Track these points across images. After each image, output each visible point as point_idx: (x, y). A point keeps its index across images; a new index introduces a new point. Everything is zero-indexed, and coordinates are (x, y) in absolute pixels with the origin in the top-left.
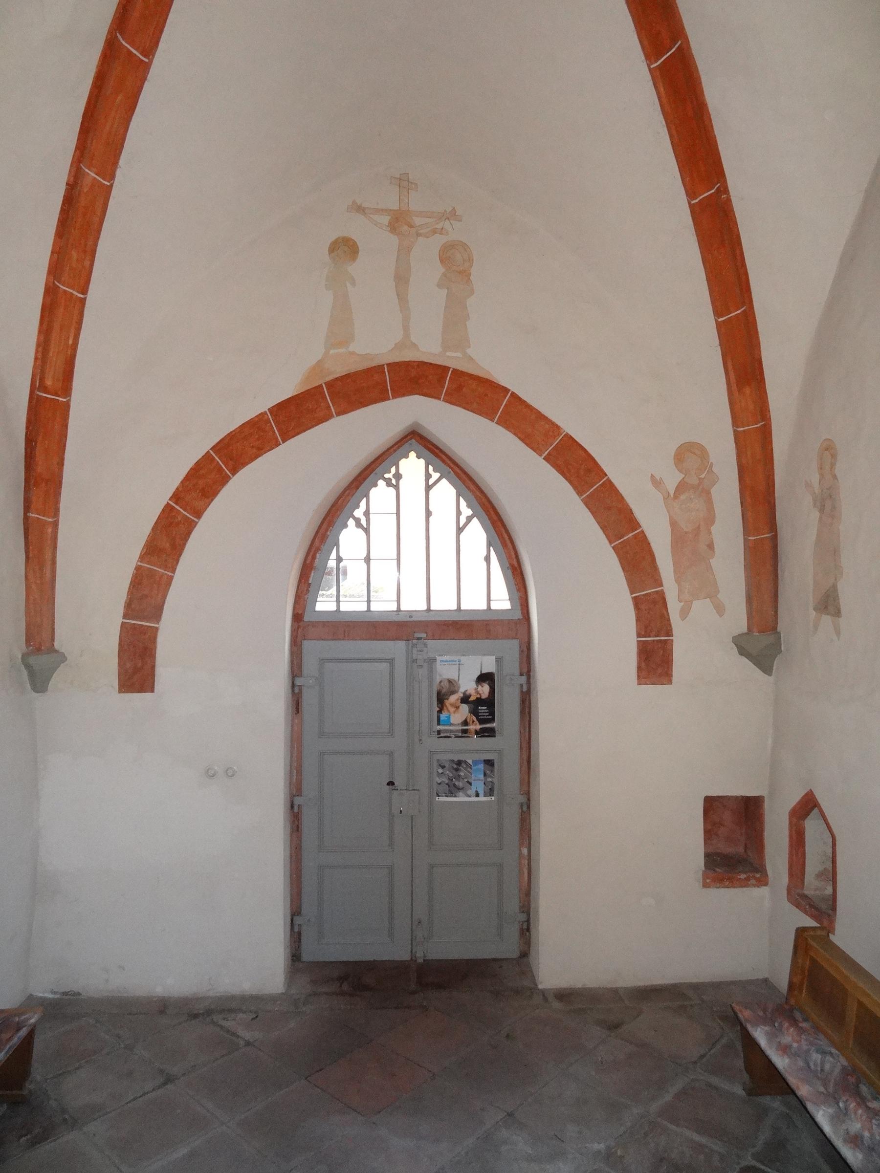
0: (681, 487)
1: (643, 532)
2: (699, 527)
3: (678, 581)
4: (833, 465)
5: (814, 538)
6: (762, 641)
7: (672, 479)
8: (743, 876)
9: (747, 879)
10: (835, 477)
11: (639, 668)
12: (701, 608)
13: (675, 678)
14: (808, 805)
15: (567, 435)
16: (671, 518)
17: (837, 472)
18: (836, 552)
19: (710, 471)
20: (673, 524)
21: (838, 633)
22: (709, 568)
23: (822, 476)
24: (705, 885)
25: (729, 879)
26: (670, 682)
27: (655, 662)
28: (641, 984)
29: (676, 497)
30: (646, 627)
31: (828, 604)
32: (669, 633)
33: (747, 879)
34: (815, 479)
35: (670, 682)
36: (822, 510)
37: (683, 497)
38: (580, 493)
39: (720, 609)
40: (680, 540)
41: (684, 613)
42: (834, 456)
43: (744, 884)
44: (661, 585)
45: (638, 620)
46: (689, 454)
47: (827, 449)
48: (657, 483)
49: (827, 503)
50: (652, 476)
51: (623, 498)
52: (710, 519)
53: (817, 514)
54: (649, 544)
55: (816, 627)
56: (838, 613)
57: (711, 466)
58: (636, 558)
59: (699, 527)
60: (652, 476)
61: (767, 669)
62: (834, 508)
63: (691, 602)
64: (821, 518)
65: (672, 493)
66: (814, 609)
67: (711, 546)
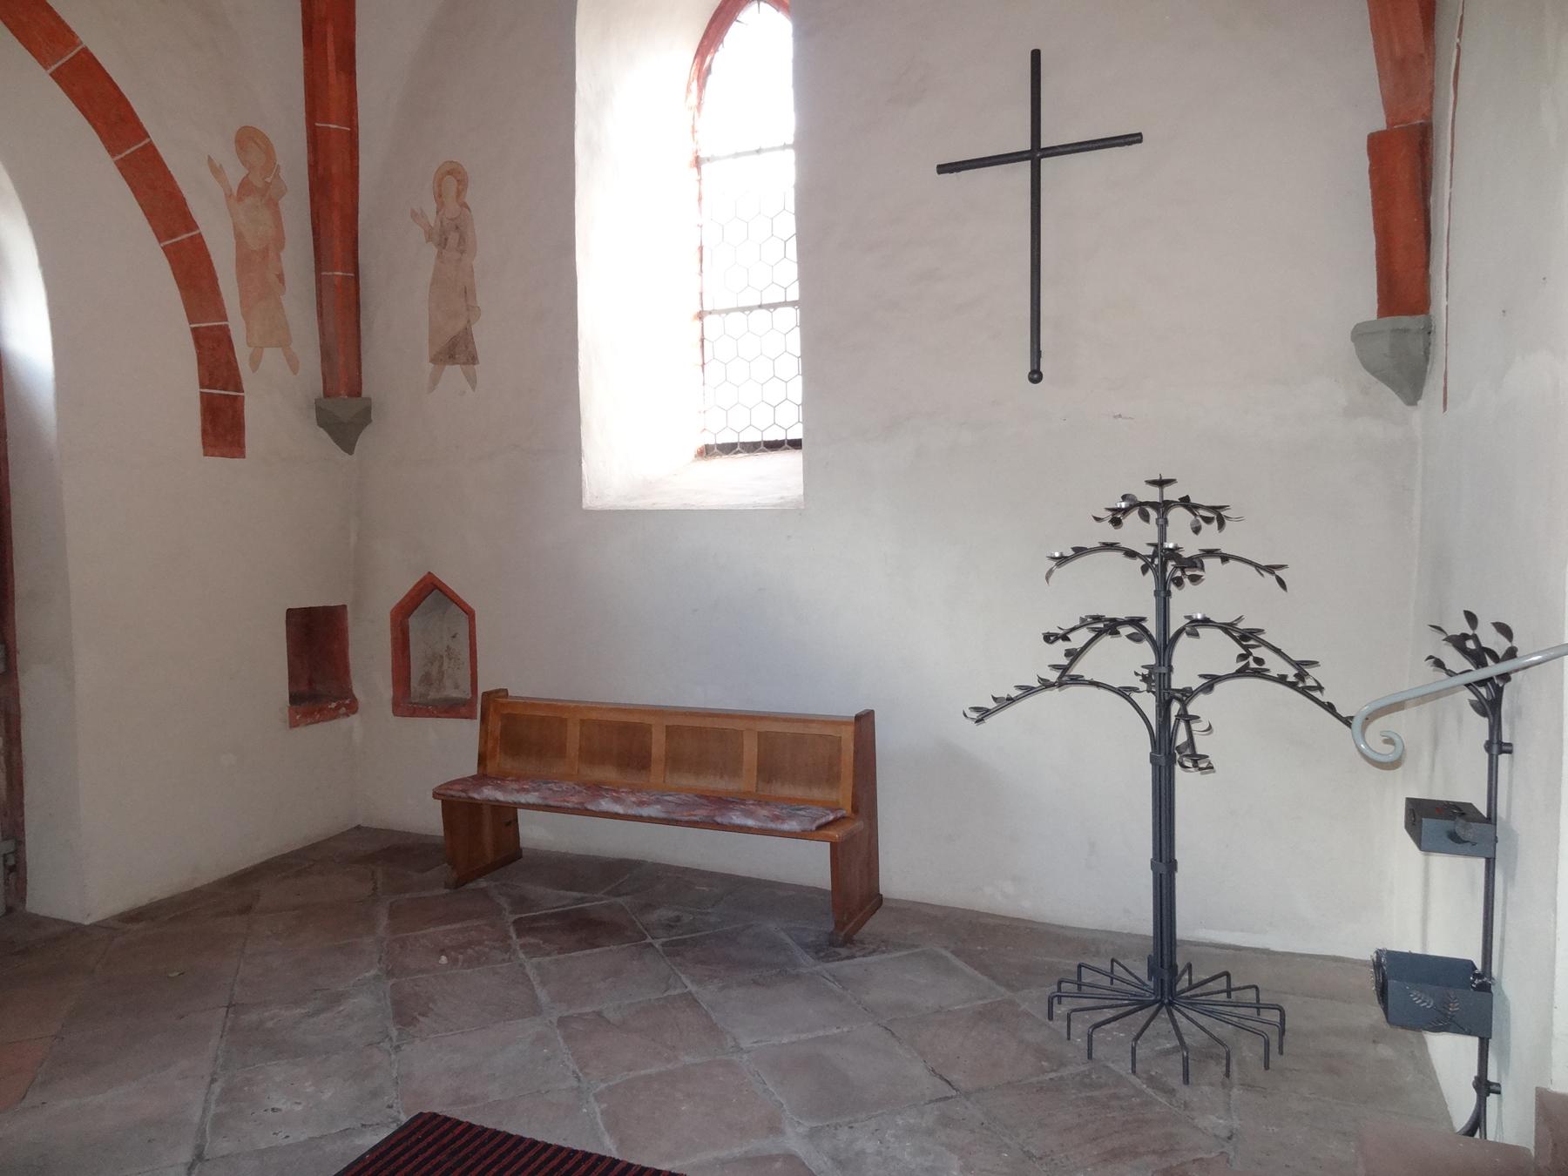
0: (245, 187)
1: (200, 235)
2: (267, 249)
3: (246, 315)
4: (459, 193)
5: (430, 275)
6: (344, 410)
7: (236, 173)
8: (333, 705)
9: (337, 708)
10: (465, 205)
11: (204, 432)
12: (272, 358)
13: (248, 451)
14: (429, 591)
15: (85, 50)
17: (469, 198)
18: (468, 292)
19: (277, 176)
20: (239, 236)
21: (472, 381)
22: (280, 306)
23: (441, 205)
24: (294, 724)
25: (320, 711)
26: (242, 455)
27: (223, 426)
28: (225, 874)
29: (240, 199)
31: (456, 350)
32: (239, 388)
33: (337, 708)
34: (430, 208)
35: (242, 455)
36: (443, 244)
37: (248, 201)
38: (112, 151)
39: (293, 364)
40: (245, 261)
41: (255, 363)
42: (462, 183)
43: (334, 715)
46: (249, 140)
47: (449, 173)
48: (217, 171)
49: (452, 236)
52: (279, 241)
53: (432, 250)
55: (434, 381)
56: (473, 359)
58: (192, 269)
59: (267, 249)
61: (348, 447)
62: (462, 240)
64: (439, 255)
66: (433, 360)
67: (281, 278)
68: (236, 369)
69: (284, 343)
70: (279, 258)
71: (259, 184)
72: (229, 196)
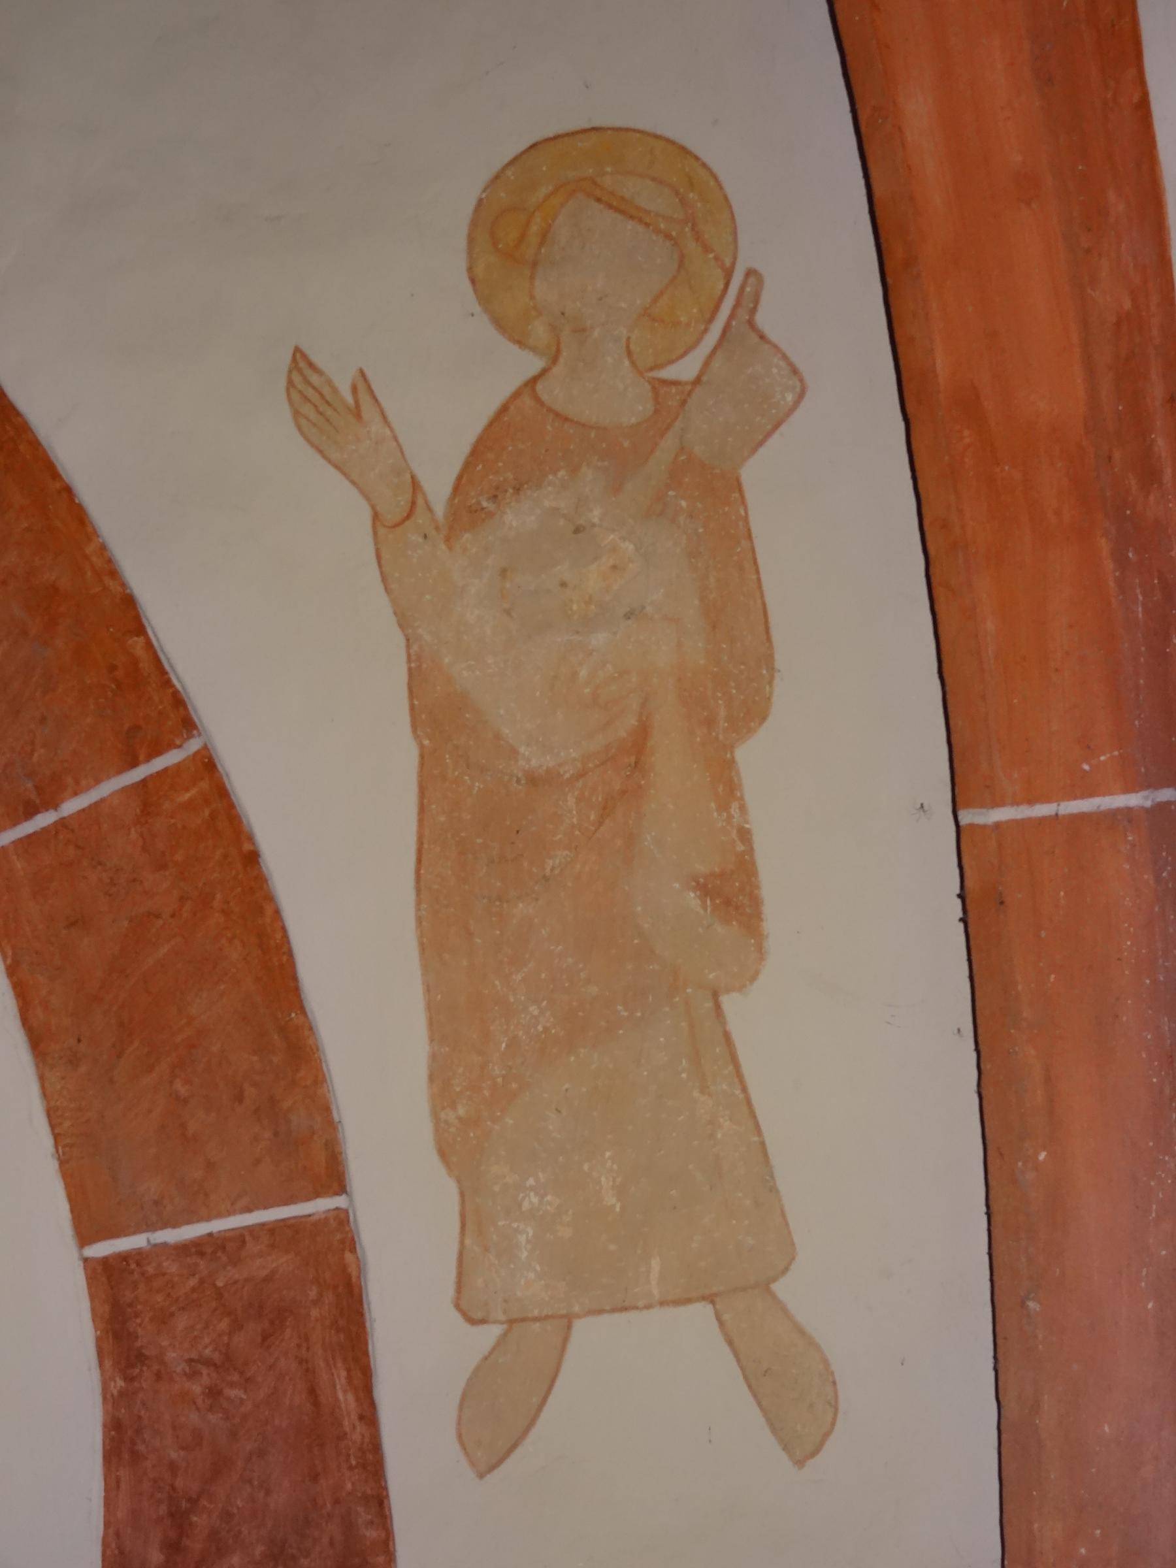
0: (510, 451)
1: (207, 764)
2: (638, 744)
3: (458, 1149)
16: (419, 676)
19: (745, 332)
20: (441, 717)
30: (179, 1519)
37: (519, 518)
39: (793, 1396)
40: (481, 836)
41: (498, 1418)
44: (334, 1179)
45: (122, 1445)
50: (300, 361)
51: (79, 515)
52: (733, 687)
54: (252, 858)
57: (749, 302)
60: (300, 361)
63: (568, 1321)
65: (438, 489)
67: (733, 893)
68: (372, 1462)
69: (740, 1283)
70: (726, 784)
71: (612, 395)
72: (395, 518)
